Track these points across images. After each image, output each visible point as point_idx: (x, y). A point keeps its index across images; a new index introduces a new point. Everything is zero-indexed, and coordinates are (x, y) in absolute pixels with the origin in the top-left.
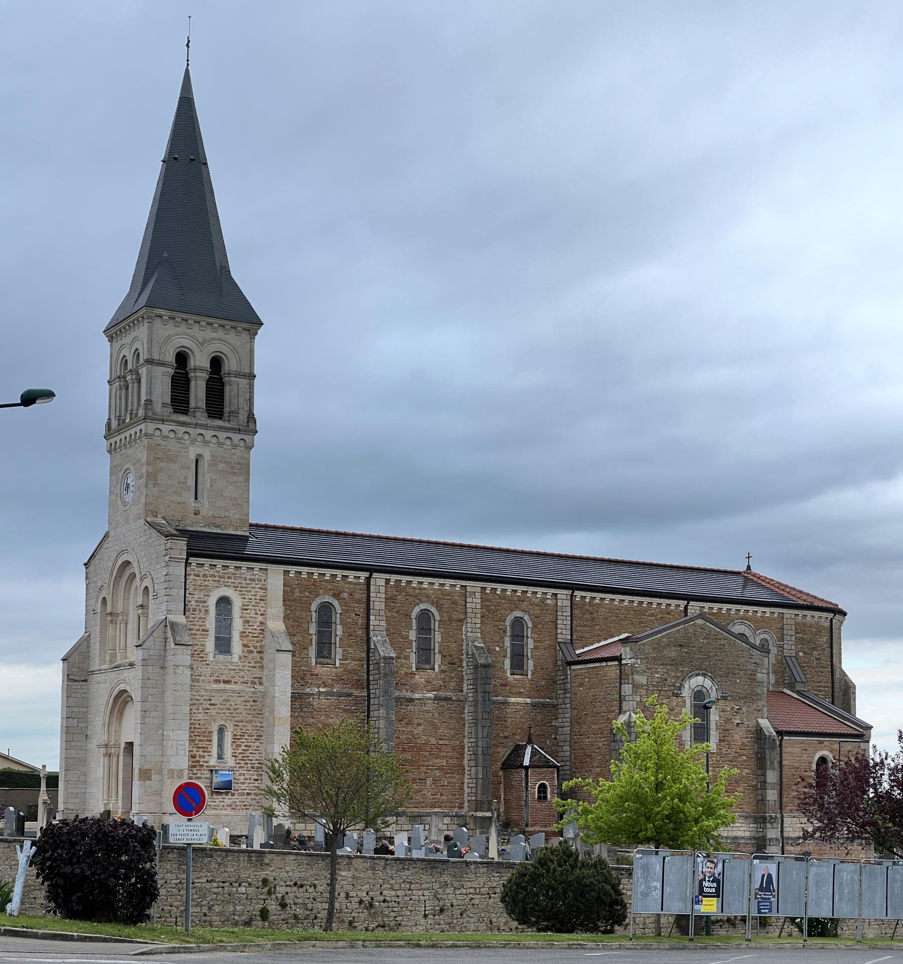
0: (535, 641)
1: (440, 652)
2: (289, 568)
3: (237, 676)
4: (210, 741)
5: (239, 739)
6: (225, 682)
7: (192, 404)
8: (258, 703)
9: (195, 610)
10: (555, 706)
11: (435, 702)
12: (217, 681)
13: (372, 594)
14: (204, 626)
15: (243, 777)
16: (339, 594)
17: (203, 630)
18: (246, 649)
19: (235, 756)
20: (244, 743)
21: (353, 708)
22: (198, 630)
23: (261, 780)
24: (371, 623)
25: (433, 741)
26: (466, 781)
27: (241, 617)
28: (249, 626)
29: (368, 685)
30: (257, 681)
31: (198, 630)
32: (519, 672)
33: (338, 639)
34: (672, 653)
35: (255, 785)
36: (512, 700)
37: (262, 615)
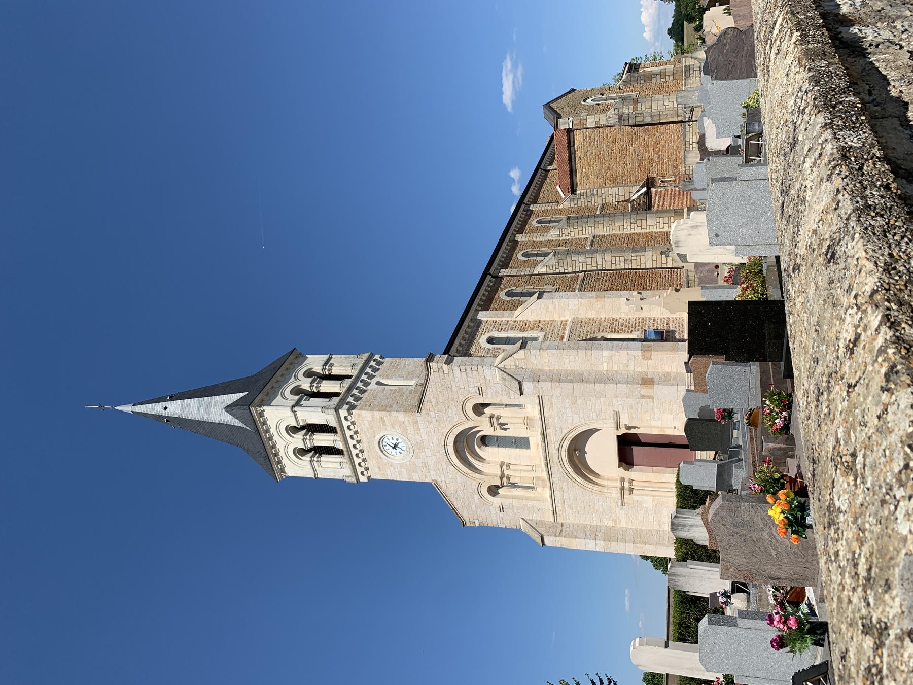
19: (631, 332)
20: (619, 328)
29: (575, 273)
35: (659, 321)
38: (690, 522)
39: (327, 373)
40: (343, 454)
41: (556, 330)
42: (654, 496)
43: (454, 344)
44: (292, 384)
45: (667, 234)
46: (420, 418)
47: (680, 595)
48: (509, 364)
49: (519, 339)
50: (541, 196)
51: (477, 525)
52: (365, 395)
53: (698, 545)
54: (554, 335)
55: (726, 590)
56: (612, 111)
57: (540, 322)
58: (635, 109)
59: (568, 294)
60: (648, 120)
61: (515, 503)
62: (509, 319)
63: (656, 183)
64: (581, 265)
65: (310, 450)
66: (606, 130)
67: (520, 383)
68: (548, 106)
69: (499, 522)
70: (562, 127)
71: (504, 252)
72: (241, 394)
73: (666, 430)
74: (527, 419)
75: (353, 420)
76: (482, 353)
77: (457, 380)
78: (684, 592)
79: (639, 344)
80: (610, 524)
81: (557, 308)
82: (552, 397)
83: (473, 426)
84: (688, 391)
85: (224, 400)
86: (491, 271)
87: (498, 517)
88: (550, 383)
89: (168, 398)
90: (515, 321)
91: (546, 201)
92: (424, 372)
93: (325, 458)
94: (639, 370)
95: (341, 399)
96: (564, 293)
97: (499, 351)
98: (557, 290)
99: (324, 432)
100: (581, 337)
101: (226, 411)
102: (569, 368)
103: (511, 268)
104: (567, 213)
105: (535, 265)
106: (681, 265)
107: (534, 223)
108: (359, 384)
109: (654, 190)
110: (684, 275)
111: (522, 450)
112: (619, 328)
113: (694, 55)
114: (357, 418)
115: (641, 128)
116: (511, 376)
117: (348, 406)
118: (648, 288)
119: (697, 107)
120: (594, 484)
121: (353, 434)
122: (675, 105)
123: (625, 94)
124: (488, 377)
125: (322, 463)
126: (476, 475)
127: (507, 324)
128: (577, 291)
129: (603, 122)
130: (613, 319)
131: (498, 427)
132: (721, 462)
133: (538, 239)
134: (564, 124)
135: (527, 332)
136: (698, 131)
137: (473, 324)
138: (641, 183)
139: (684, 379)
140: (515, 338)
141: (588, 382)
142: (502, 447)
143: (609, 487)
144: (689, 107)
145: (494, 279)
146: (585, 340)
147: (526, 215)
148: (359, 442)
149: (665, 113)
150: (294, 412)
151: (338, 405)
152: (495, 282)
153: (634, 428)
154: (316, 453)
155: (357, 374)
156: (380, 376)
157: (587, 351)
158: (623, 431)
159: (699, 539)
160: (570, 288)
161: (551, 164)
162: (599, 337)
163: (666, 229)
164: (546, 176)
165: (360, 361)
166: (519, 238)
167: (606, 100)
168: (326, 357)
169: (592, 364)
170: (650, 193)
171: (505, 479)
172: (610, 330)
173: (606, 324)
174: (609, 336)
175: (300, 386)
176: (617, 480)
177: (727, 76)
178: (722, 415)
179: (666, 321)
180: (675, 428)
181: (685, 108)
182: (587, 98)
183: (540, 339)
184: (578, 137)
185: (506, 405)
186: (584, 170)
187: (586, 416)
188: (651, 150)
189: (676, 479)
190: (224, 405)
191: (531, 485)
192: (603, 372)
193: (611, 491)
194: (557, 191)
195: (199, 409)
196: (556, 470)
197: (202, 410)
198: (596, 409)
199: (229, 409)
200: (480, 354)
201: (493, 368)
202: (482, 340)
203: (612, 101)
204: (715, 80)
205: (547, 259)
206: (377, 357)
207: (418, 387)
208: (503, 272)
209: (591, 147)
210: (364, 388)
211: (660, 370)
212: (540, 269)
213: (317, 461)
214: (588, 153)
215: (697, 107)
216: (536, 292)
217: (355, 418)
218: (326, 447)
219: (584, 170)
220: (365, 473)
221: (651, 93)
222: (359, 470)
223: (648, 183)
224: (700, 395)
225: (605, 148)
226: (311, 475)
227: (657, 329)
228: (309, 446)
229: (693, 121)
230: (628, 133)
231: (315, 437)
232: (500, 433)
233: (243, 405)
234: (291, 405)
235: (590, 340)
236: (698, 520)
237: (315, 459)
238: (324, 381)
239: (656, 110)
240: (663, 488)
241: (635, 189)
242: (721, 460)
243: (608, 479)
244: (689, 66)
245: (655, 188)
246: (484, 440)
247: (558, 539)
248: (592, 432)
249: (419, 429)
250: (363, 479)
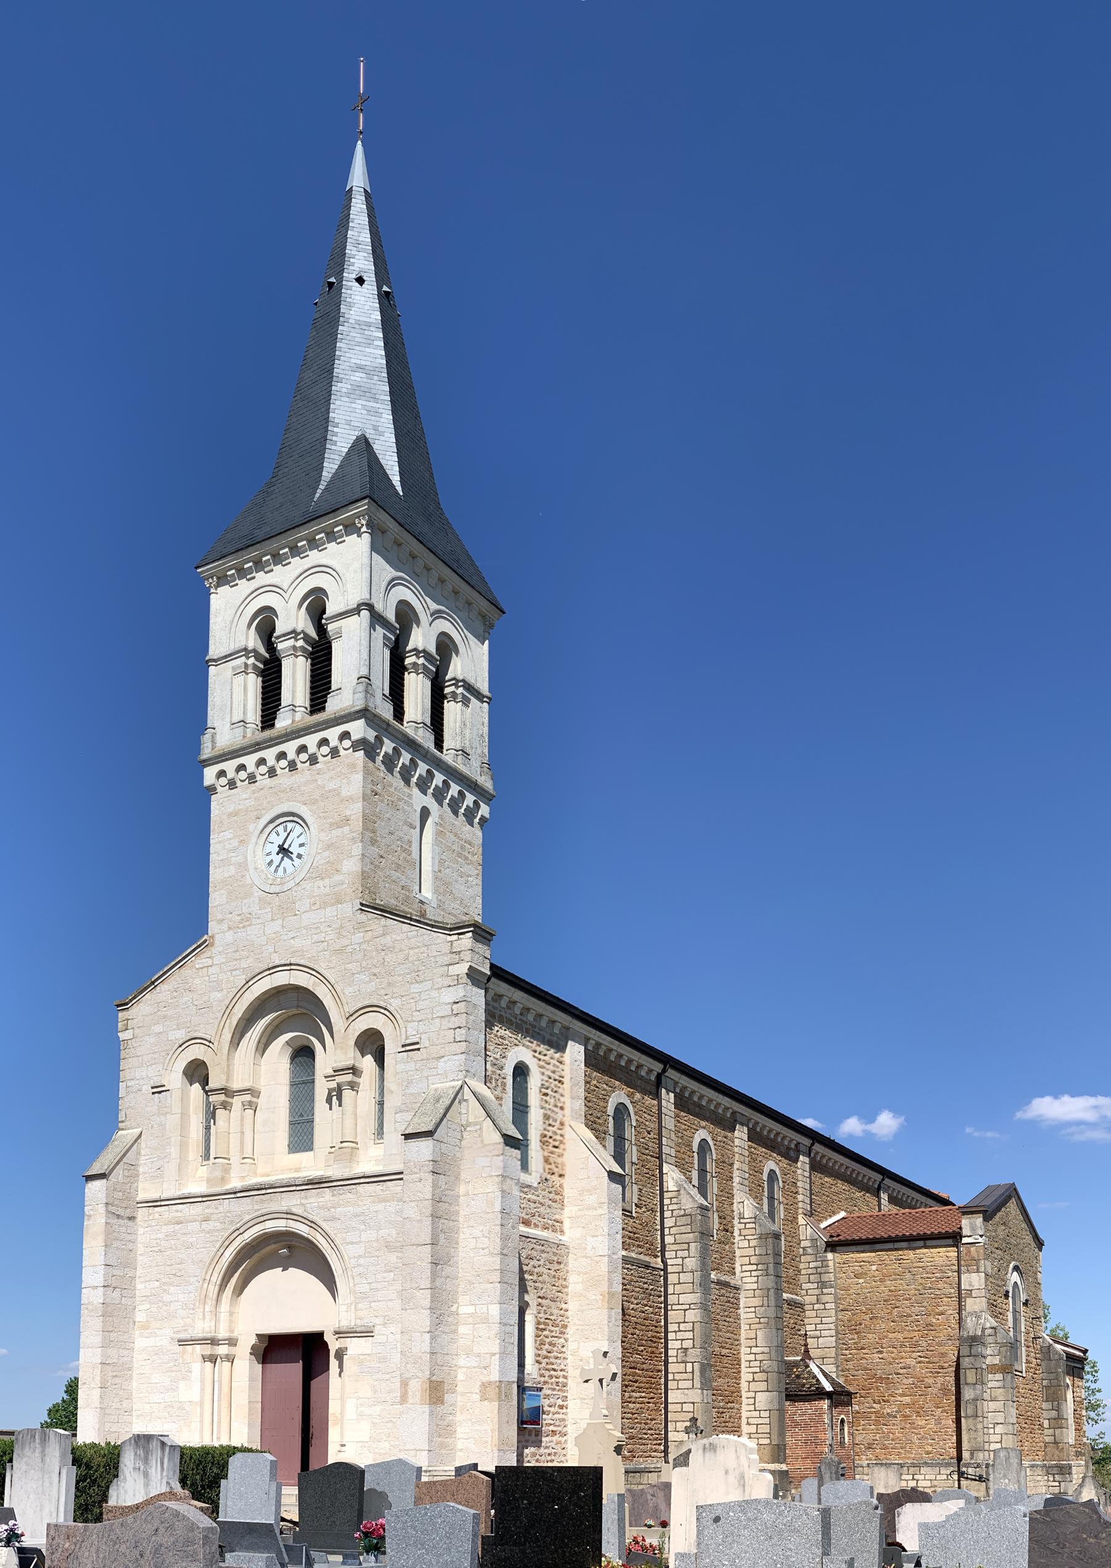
3: (537, 1214)
8: (562, 1266)
11: (717, 1287)
18: (548, 1166)
19: (537, 1362)
20: (547, 1337)
21: (651, 1287)
26: (744, 1414)
28: (550, 1125)
35: (561, 1416)
38: (155, 1472)
39: (447, 690)
40: (263, 728)
41: (542, 1210)
42: (201, 1403)
43: (513, 989)
44: (423, 605)
45: (736, 1430)
46: (349, 908)
47: (5, 1453)
48: (471, 1111)
49: (524, 1131)
50: (826, 1179)
51: (122, 1036)
52: (397, 781)
53: (108, 1488)
54: (533, 1205)
55: (23, 1538)
56: (991, 1322)
57: (561, 1176)
58: (993, 1369)
59: (619, 1236)
60: (968, 1394)
61: (173, 1121)
62: (567, 1111)
63: (840, 1409)
64: (679, 1261)
65: (270, 647)
66: (952, 1312)
67: (429, 1134)
68: (1011, 1193)
69: (129, 1084)
70: (965, 1222)
71: (710, 1101)
72: (398, 478)
73: (338, 1428)
74: (352, 1148)
75: (342, 752)
76: (494, 1053)
77: (435, 994)
78: (11, 1461)
79: (513, 1376)
80: (140, 1317)
81: (589, 1213)
82: (401, 1200)
83: (335, 1029)
84: (419, 1469)
85: (382, 434)
86: (671, 1073)
87: (141, 1082)
88: (429, 1196)
89: (385, 288)
90: (562, 1124)
91: (815, 1189)
92: (450, 920)
93: (254, 683)
94: (461, 1376)
95: (388, 724)
96: (621, 1227)
97: (499, 1089)
98: (627, 1213)
99: (312, 682)
100: (527, 1261)
101: (358, 438)
102: (462, 1236)
103: (677, 1116)
104: (787, 1233)
105: (682, 1166)
106: (671, 1457)
107: (770, 1165)
108: (422, 768)
109: (826, 1406)
110: (650, 1464)
111: (287, 1135)
112: (547, 1337)
113: (1089, 1481)
114: (347, 761)
115: (952, 1380)
116: (445, 1115)
117: (372, 740)
118: (627, 1394)
119: (987, 1489)
120: (221, 1285)
121: (310, 751)
122: (994, 1446)
123: (1024, 1349)
124: (441, 1063)
125: (241, 678)
126: (227, 1036)
127: (556, 1106)
128: (624, 1253)
129: (971, 1305)
130: (565, 1327)
131: (333, 1085)
132: (277, 1532)
133: (736, 1173)
134: (972, 1228)
135: (539, 1148)
136: (939, 1490)
137: (556, 1031)
138: (841, 1381)
139: (442, 1463)
140: (526, 1124)
141: (434, 1276)
142: (291, 1093)
143: (216, 1313)
144: (988, 1474)
145: (653, 1078)
146: (521, 1272)
147: (789, 1148)
148: (292, 766)
149: (980, 1426)
150: (357, 611)
151: (375, 716)
152: (648, 1081)
153: (341, 1366)
154: (266, 662)
155: (444, 762)
156: (441, 817)
157: (498, 1274)
158: (333, 1345)
159: (122, 1491)
160: (631, 1239)
161: (892, 1200)
162: (527, 1298)
163: (745, 1429)
164: (865, 1188)
165: (474, 769)
166: (741, 1134)
167: (1015, 1311)
168: (484, 687)
169: (471, 1283)
170: (821, 1399)
171: (222, 1097)
172: (542, 1320)
173: (555, 1311)
174: (529, 1319)
175: (418, 626)
176: (232, 1331)
177: (1035, 1540)
178: (371, 1533)
179: (559, 1429)
180: (343, 1445)
181: (987, 1466)
182: (1021, 1273)
183: (524, 1178)
184: (943, 1255)
185: (381, 1104)
186: (874, 1268)
187: (361, 1269)
188: (907, 1399)
189: (239, 1445)
190: (370, 435)
191: (212, 1155)
192: (455, 1306)
193: (208, 1317)
194: (834, 1213)
195: (360, 368)
196: (246, 1208)
197: (358, 377)
198: (377, 1290)
199: (363, 446)
200: (491, 1047)
201: (461, 1075)
202: (523, 1052)
203: (1010, 1323)
204: (1031, 1519)
205: (694, 1192)
206: (484, 810)
207: (416, 906)
208: (668, 1099)
209: (920, 1281)
210: (414, 780)
211: (459, 1417)
212: (672, 1177)
213: (246, 665)
214: (908, 1276)
215: (987, 1489)
216: (623, 1167)
217: (346, 756)
218: (280, 688)
219: (874, 1268)
220: (223, 781)
221: (1021, 1399)
222: (230, 766)
223: (841, 1393)
224: (410, 1494)
225: (917, 1309)
226: (215, 651)
227: (544, 1413)
228: (280, 646)
229: (959, 1481)
230: (943, 1355)
231: (301, 659)
232: (322, 1088)
233: (371, 482)
234: (374, 601)
235: (522, 1281)
236: (158, 1486)
237: (252, 661)
238: (428, 684)
239: (986, 1410)
240: (219, 1422)
241: (830, 1369)
242: (281, 1533)
243: (231, 1314)
244: (1070, 1473)
245: (830, 1407)
246: (303, 1055)
247: (102, 1209)
248: (328, 1280)
249: (324, 905)
250: (209, 775)
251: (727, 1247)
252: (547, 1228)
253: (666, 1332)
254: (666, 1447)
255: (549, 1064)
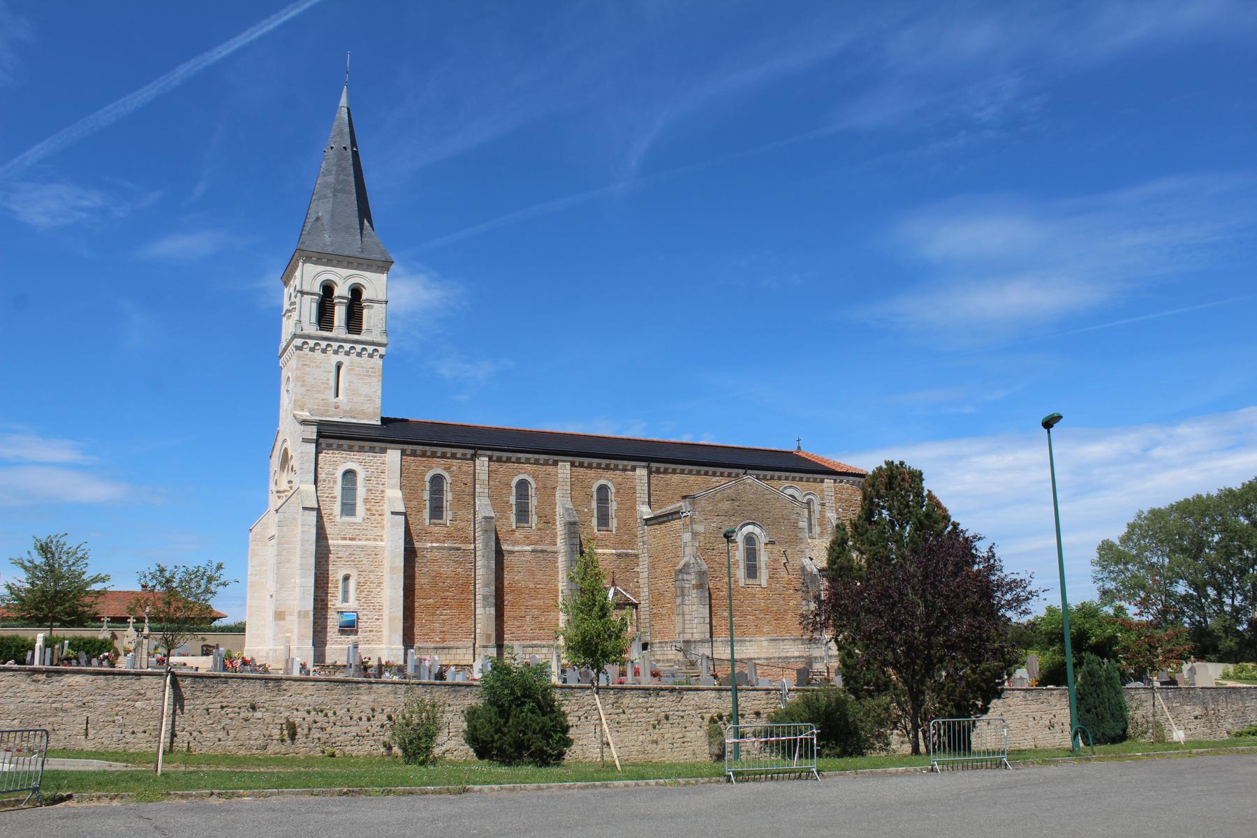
0: (618, 504)
1: (536, 513)
2: (406, 447)
4: (337, 587)
5: (362, 586)
6: (351, 539)
7: (336, 323)
9: (325, 481)
10: (636, 556)
12: (344, 539)
13: (476, 468)
14: (333, 493)
15: (365, 617)
16: (449, 468)
17: (332, 497)
18: (368, 513)
22: (327, 497)
23: (382, 619)
24: (477, 490)
25: (532, 585)
27: (365, 487)
29: (475, 540)
30: (378, 538)
31: (327, 497)
32: (605, 528)
33: (448, 504)
34: (726, 505)
36: (600, 551)
37: (382, 484)
41: (365, 532)
127: (378, 484)
173: (373, 577)
251: (548, 532)
252: (370, 540)
253: (475, 580)
254: (475, 636)
255: (373, 466)
